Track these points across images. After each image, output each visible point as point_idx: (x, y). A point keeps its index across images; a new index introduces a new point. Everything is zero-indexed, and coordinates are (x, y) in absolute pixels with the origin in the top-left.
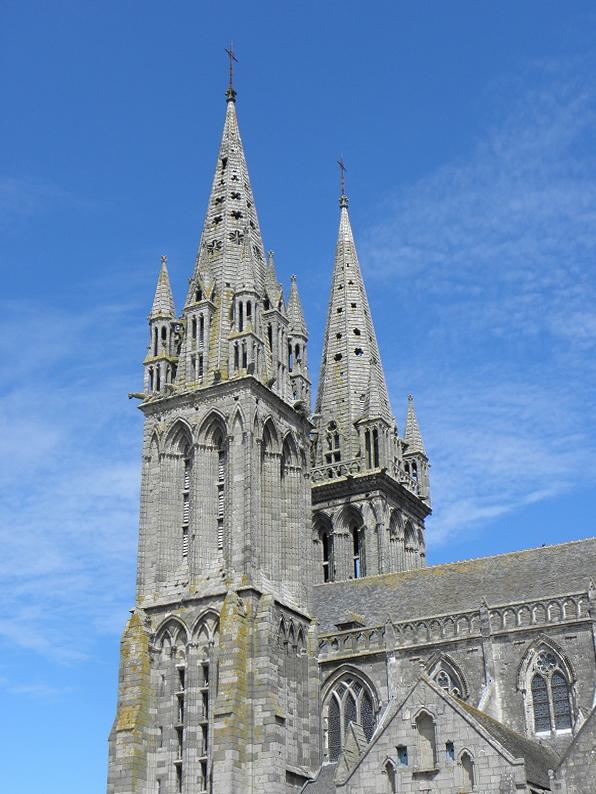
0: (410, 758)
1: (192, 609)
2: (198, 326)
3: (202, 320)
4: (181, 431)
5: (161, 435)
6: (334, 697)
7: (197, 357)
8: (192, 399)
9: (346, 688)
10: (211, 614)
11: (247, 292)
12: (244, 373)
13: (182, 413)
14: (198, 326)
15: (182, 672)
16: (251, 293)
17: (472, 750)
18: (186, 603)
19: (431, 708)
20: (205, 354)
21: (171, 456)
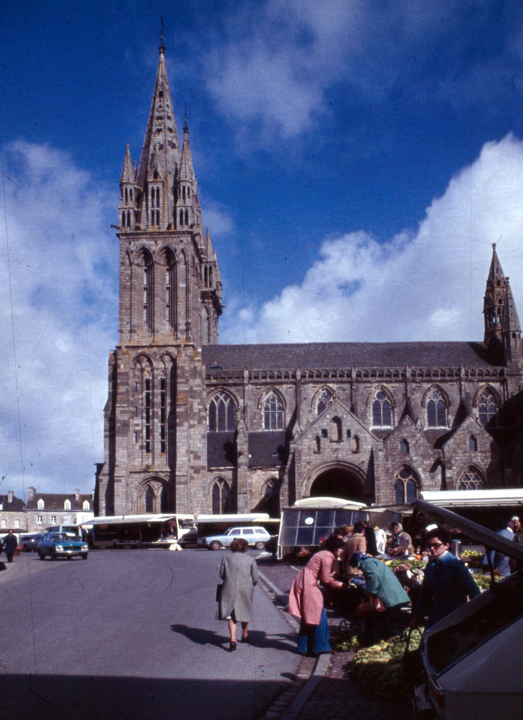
0: (329, 435)
1: (155, 349)
2: (156, 194)
3: (158, 190)
4: (146, 253)
5: (132, 252)
6: (212, 401)
7: (155, 212)
8: (152, 236)
9: (219, 398)
10: (168, 354)
11: (188, 181)
12: (186, 228)
13: (144, 242)
14: (156, 194)
15: (148, 381)
16: (190, 182)
17: (359, 434)
18: (151, 346)
19: (340, 415)
20: (161, 212)
21: (138, 265)
